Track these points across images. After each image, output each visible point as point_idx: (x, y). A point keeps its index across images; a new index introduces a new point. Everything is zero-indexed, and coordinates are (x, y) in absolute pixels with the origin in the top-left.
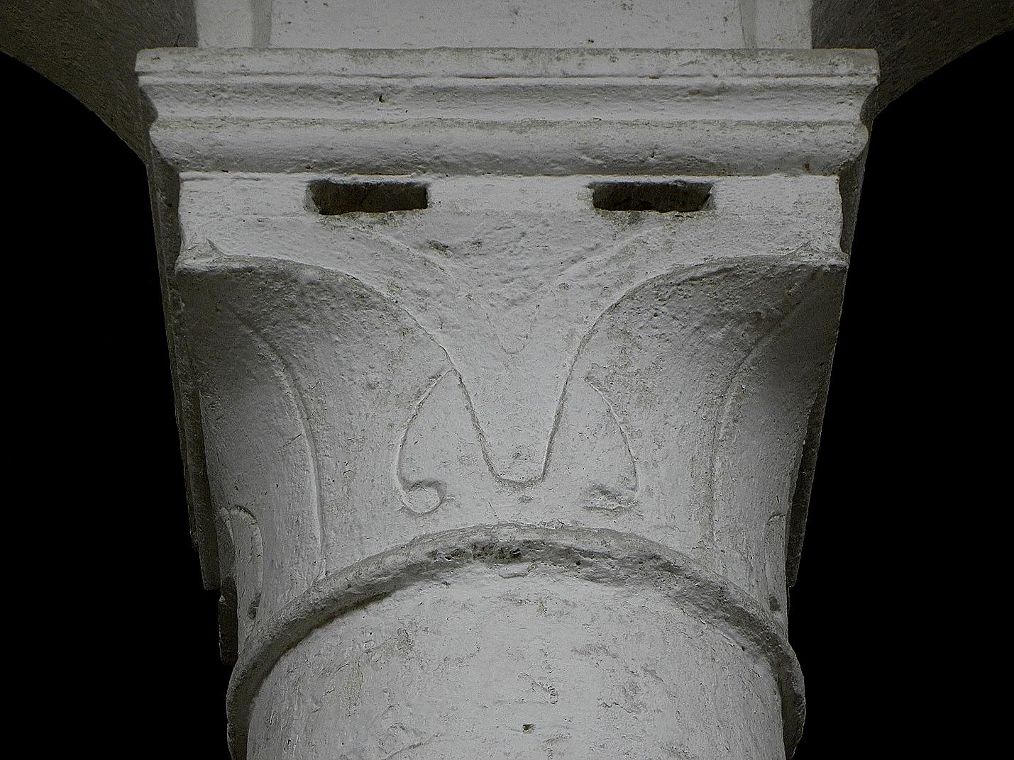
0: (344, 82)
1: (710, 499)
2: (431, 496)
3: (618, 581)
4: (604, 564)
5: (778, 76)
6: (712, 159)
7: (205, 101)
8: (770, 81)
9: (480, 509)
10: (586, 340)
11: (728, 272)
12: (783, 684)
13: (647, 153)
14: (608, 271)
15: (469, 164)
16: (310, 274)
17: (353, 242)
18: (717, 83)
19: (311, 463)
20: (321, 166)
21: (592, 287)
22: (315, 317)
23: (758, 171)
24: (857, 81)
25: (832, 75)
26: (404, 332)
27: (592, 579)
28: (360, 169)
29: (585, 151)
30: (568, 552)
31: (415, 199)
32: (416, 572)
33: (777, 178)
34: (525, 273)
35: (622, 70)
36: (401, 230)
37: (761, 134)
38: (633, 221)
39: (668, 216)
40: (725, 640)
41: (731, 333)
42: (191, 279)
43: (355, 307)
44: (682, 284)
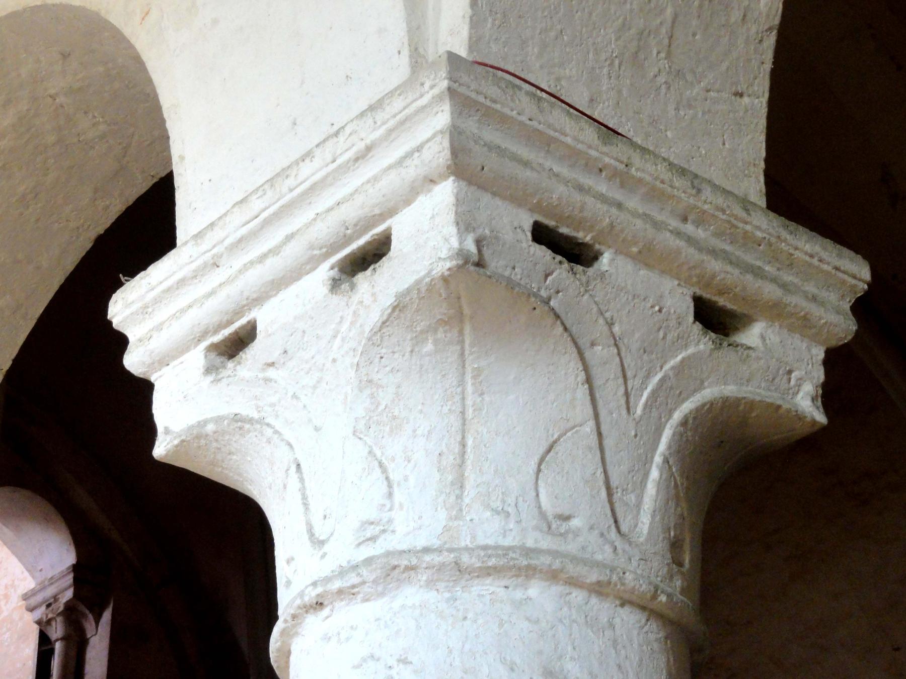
0: (193, 266)
3: (382, 594)
4: (366, 589)
5: (394, 116)
6: (377, 211)
7: (144, 319)
8: (392, 123)
13: (343, 229)
14: (351, 335)
16: (210, 428)
17: (230, 387)
18: (361, 146)
21: (347, 353)
23: (408, 202)
24: (436, 91)
25: (422, 96)
27: (366, 600)
29: (312, 247)
30: (340, 592)
33: (421, 198)
34: (314, 360)
35: (310, 171)
37: (393, 175)
41: (436, 342)
43: (243, 435)
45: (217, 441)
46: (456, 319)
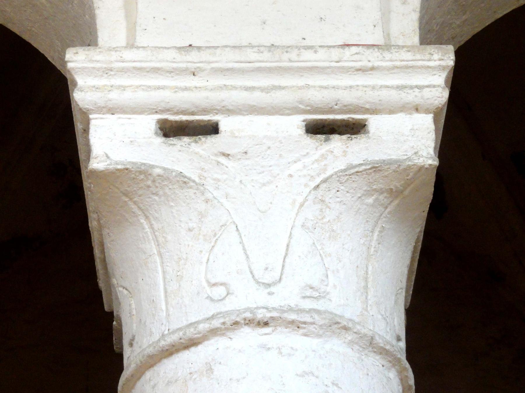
0: (175, 65)
1: (366, 287)
2: (221, 291)
3: (319, 336)
4: (312, 328)
6: (367, 106)
7: (102, 76)
8: (398, 64)
9: (247, 298)
10: (302, 205)
11: (376, 168)
12: (403, 380)
13: (334, 103)
14: (313, 167)
15: (240, 110)
16: (158, 171)
17: (180, 153)
18: (370, 65)
19: (160, 269)
20: (162, 111)
21: (305, 176)
22: (161, 193)
23: (391, 112)
24: (443, 63)
25: (429, 60)
26: (207, 201)
27: (306, 335)
28: (184, 113)
29: (301, 102)
30: (293, 322)
31: (213, 129)
32: (214, 332)
34: (271, 168)
35: (320, 58)
38: (326, 140)
39: (345, 137)
40: (374, 362)
41: (376, 200)
42: (95, 173)
43: (182, 188)
44: (350, 173)
45: (154, 181)
46: (393, 193)
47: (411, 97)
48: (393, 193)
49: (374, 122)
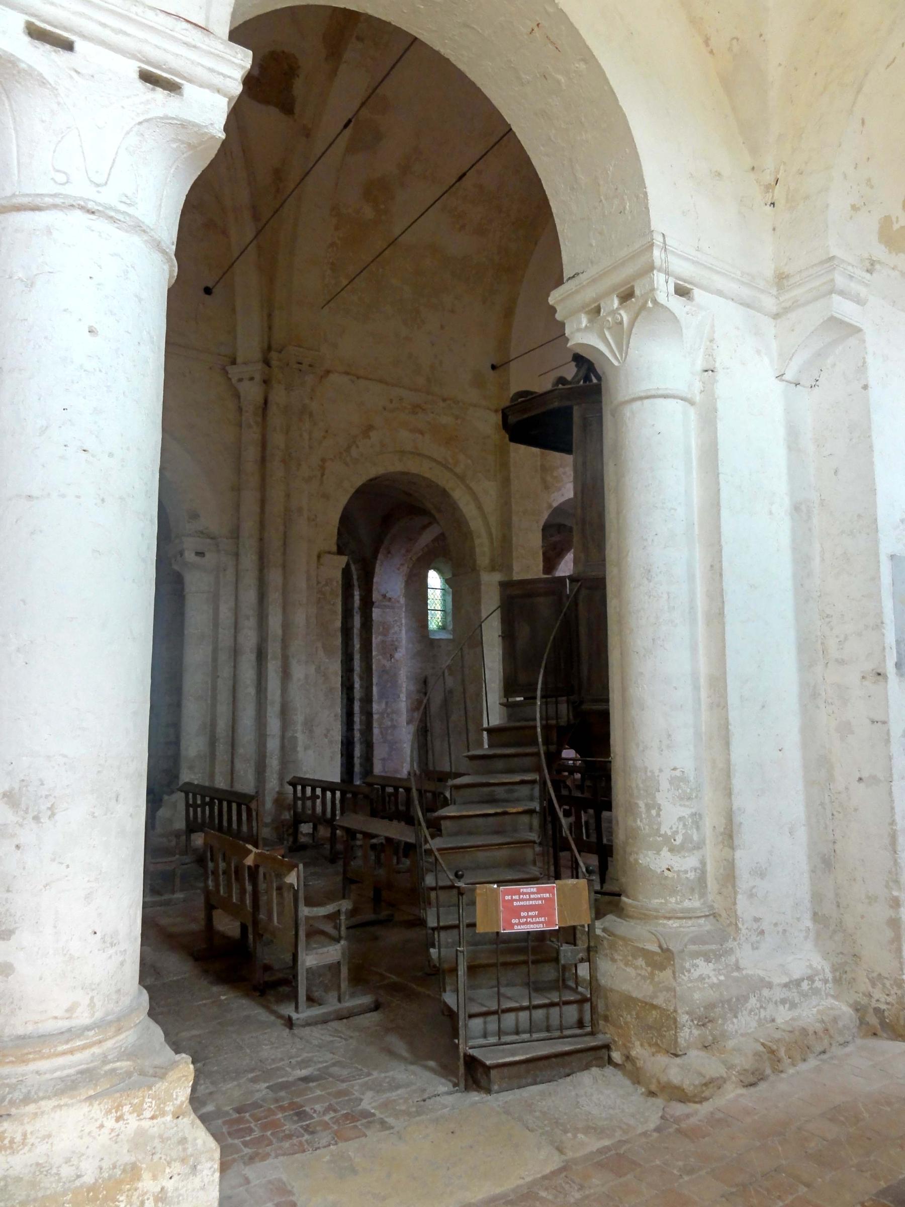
1: (160, 205)
2: (61, 178)
3: (127, 231)
4: (124, 225)
8: (213, 50)
9: (79, 189)
10: (128, 133)
11: (184, 125)
12: (171, 272)
16: (23, 65)
18: (194, 43)
19: (14, 141)
20: (32, 15)
23: (201, 86)
26: (59, 104)
30: (111, 217)
31: (68, 46)
32: (55, 206)
33: (207, 91)
36: (62, 57)
38: (153, 90)
39: (166, 92)
40: (157, 257)
44: (166, 121)
45: (19, 72)
46: (190, 146)
47: (217, 80)
48: (190, 146)
49: (188, 88)
